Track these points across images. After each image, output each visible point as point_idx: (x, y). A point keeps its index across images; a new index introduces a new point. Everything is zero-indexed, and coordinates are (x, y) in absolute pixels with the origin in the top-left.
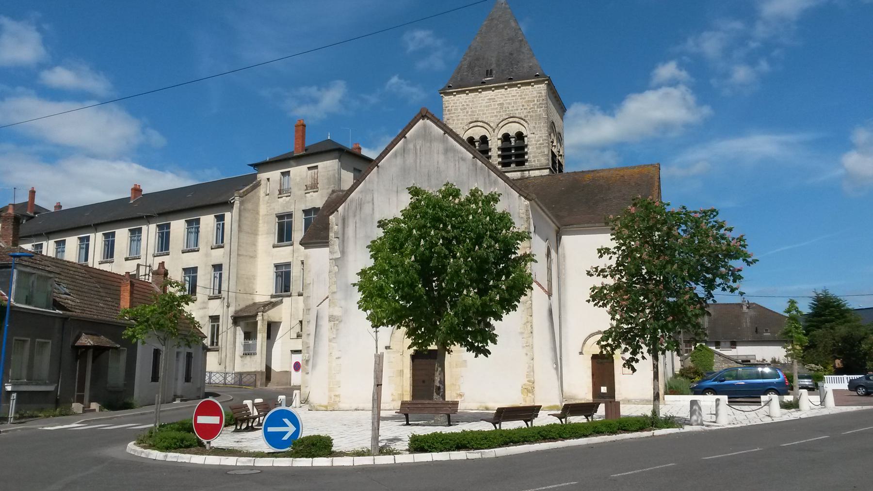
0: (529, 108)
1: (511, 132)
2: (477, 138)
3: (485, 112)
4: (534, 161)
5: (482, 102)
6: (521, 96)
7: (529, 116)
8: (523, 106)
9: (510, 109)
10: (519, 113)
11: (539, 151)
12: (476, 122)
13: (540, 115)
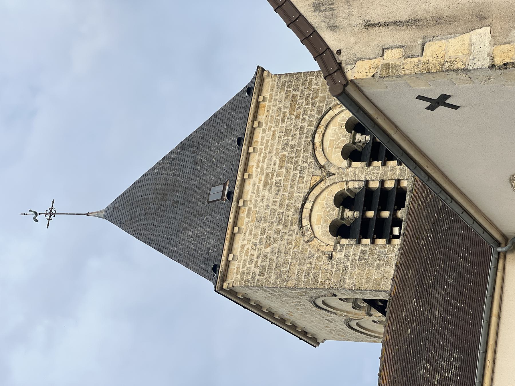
0: (304, 106)
1: (343, 141)
2: (335, 213)
3: (286, 194)
8: (297, 117)
9: (296, 143)
12: (301, 213)
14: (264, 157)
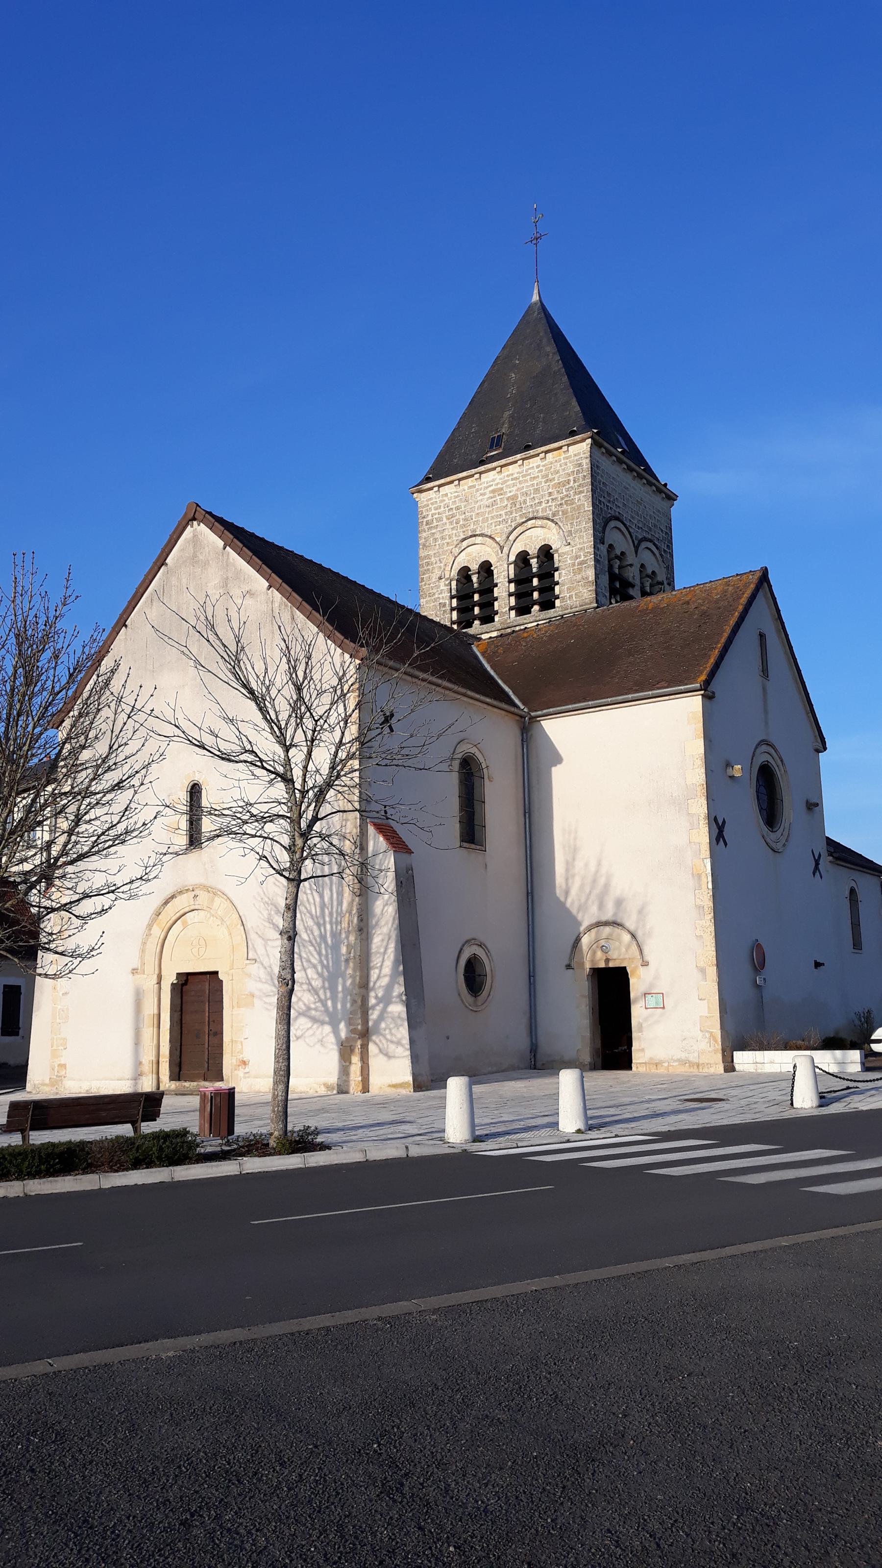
4: (571, 597)
5: (481, 497)
6: (547, 476)
7: (560, 513)
8: (550, 494)
9: (528, 504)
10: (544, 510)
11: (579, 577)
13: (579, 507)
14: (516, 479)
